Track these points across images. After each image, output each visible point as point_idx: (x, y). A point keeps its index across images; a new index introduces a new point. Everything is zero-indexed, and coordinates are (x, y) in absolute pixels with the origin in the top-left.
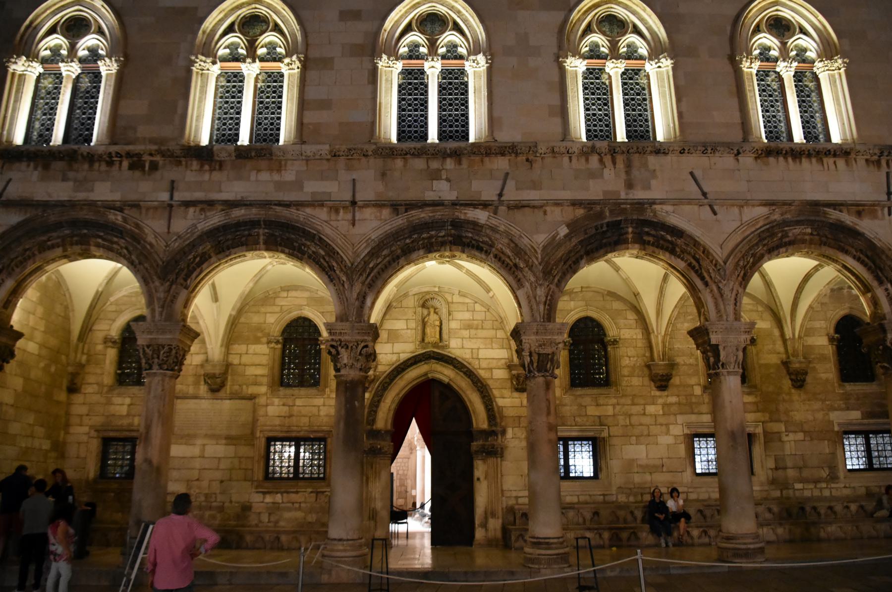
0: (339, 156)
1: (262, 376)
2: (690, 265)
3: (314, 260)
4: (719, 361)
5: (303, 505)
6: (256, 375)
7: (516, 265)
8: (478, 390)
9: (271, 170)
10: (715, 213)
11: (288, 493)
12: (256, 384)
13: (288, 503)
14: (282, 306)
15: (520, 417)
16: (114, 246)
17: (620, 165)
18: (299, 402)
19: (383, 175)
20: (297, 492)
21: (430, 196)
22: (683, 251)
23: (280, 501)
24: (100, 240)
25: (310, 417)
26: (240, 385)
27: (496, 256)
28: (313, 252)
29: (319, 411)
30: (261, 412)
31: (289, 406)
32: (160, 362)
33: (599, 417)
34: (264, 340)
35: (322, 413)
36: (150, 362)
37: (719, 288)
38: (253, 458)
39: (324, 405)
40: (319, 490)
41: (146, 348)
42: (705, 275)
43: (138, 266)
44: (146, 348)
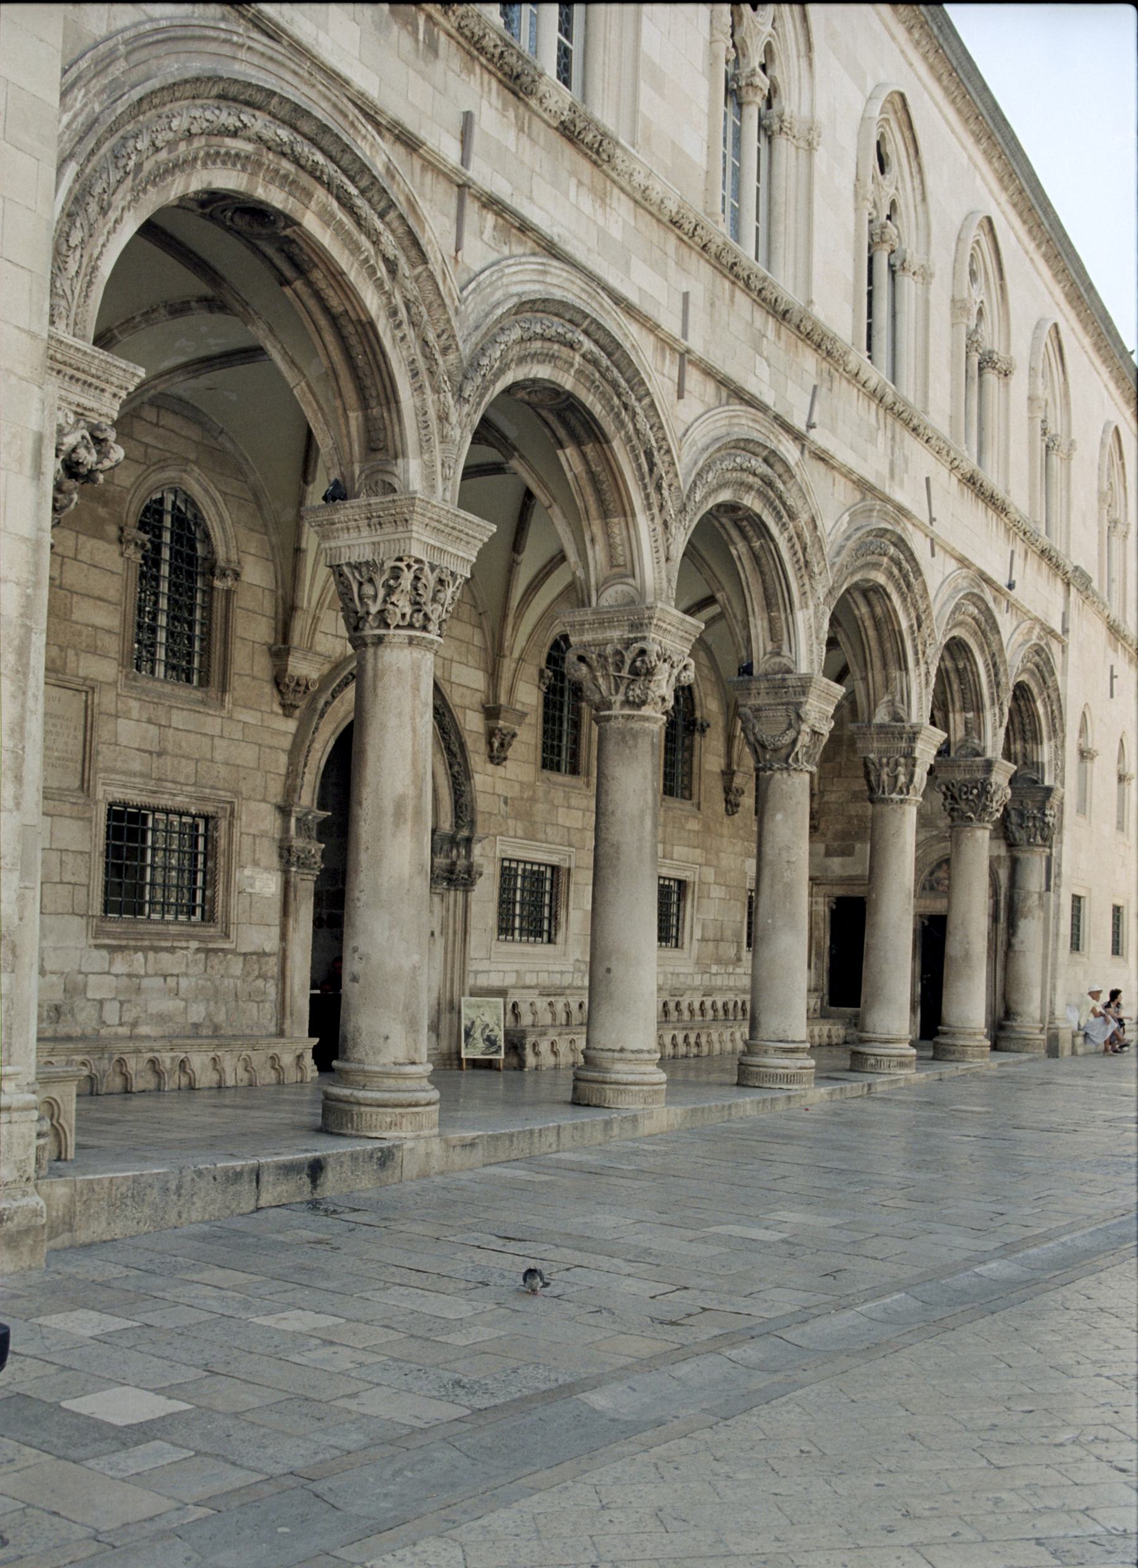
0: (680, 227)
1: (109, 632)
2: (911, 627)
3: (633, 448)
4: (911, 780)
5: (184, 983)
6: (93, 626)
7: (807, 563)
8: (448, 749)
9: (592, 190)
10: (933, 555)
11: (157, 950)
12: (93, 650)
13: (156, 975)
14: (147, 445)
15: (490, 813)
16: (363, 240)
17: (889, 435)
18: (178, 718)
19: (712, 305)
20: (171, 950)
21: (752, 386)
22: (915, 605)
23: (142, 972)
24: (335, 205)
25: (197, 761)
26: (61, 648)
27: (790, 539)
28: (637, 431)
29: (213, 748)
30: (104, 731)
31: (160, 726)
32: (444, 616)
33: (569, 828)
34: (112, 530)
35: (219, 756)
36: (428, 609)
37: (928, 673)
38: (89, 853)
39: (222, 737)
40: (211, 946)
41: (427, 568)
42: (920, 647)
43: (405, 326)
44: (427, 568)
